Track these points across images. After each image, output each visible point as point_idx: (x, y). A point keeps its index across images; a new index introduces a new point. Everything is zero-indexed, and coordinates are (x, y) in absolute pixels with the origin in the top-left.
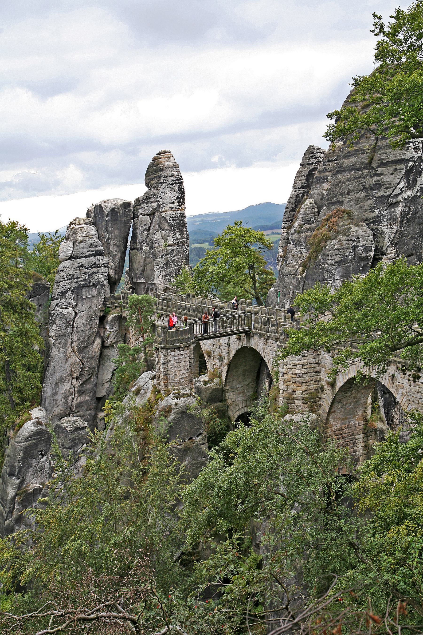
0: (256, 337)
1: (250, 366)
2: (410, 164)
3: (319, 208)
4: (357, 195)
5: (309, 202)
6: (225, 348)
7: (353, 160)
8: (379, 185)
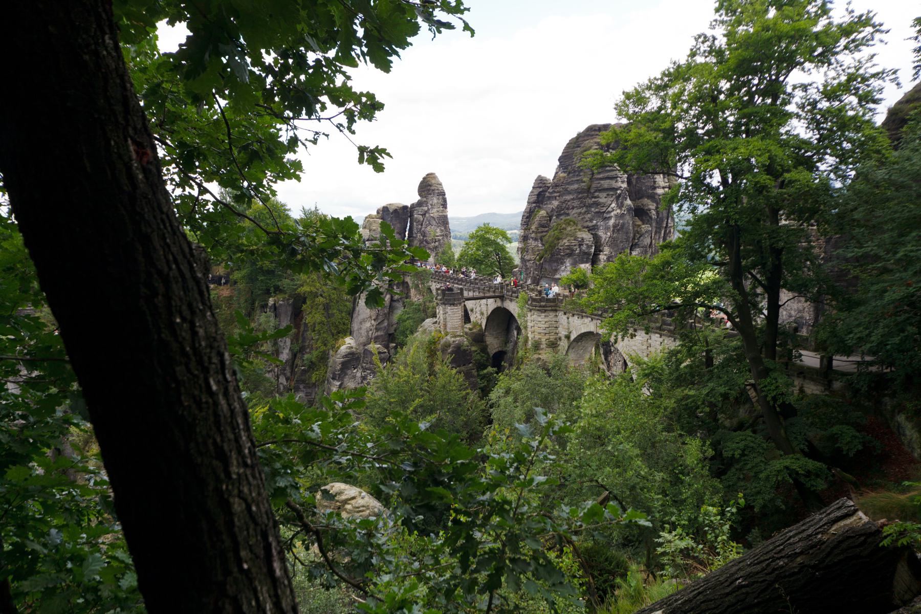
0: (508, 301)
1: (503, 321)
2: (619, 192)
3: (551, 217)
4: (579, 210)
5: (543, 213)
6: (484, 308)
7: (576, 186)
8: (597, 204)
